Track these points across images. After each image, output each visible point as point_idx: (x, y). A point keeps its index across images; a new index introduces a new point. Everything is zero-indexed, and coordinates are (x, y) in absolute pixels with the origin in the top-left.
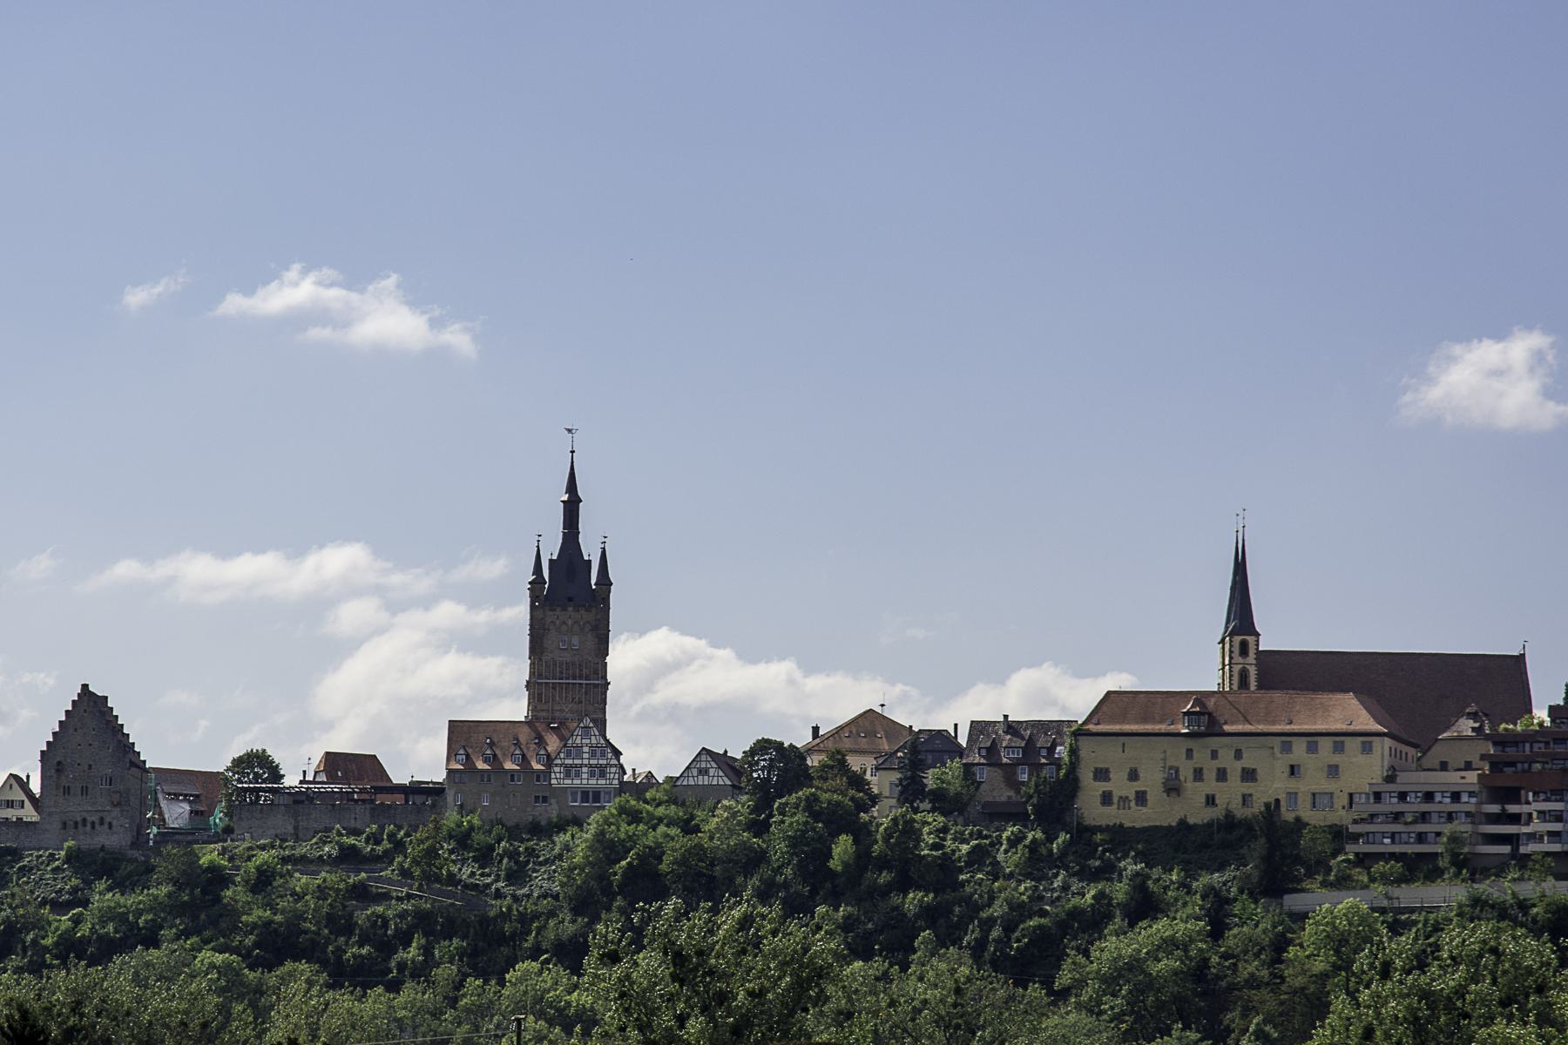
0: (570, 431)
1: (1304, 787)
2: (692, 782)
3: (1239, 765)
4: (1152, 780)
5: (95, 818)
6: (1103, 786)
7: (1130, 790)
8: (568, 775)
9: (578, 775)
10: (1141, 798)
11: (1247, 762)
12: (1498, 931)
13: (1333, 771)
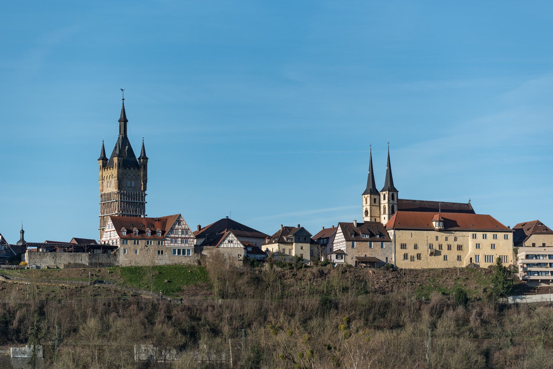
0: (122, 90)
1: (481, 254)
2: (225, 246)
3: (456, 243)
4: (424, 250)
6: (404, 251)
7: (414, 253)
8: (172, 242)
9: (176, 242)
10: (419, 256)
11: (459, 242)
12: (242, 307)
13: (493, 246)
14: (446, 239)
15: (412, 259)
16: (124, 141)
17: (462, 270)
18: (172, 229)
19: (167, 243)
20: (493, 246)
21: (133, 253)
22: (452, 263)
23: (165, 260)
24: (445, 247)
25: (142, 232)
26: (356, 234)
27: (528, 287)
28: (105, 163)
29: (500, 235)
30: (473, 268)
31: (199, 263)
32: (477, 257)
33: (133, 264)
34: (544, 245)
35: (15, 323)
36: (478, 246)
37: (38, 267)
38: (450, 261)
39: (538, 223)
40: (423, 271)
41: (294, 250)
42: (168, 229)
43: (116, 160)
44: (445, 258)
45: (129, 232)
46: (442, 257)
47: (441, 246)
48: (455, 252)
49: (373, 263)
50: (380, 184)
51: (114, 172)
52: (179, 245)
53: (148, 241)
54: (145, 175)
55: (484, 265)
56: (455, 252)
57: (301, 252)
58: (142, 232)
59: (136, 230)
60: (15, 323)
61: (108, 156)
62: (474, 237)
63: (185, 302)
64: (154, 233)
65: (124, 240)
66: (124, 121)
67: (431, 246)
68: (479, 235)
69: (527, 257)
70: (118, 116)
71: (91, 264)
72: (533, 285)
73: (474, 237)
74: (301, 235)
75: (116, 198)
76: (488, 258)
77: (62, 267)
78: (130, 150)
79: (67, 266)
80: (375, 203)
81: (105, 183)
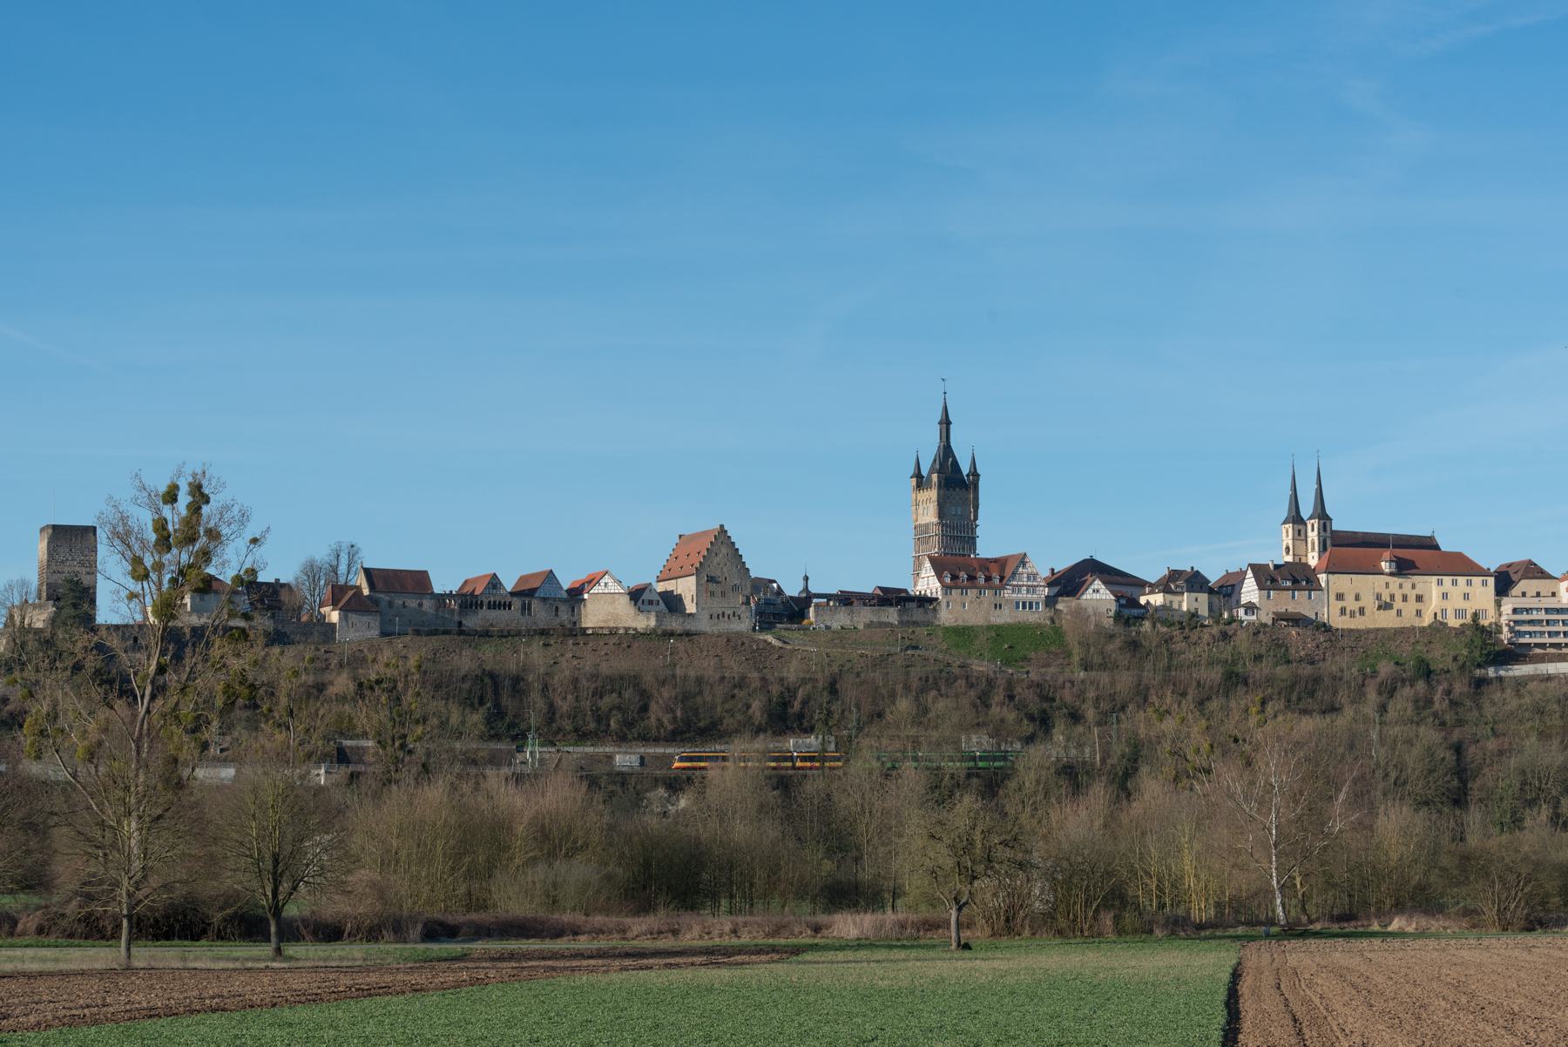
3: (1414, 592)
4: (1369, 602)
5: (728, 612)
6: (1341, 604)
7: (1355, 606)
10: (1362, 611)
11: (1418, 591)
12: (1113, 683)
13: (1466, 596)
14: (1401, 586)
15: (1352, 614)
16: (946, 451)
17: (1422, 630)
18: (1014, 574)
20: (1466, 596)
21: (960, 608)
22: (1409, 619)
23: (1004, 617)
24: (1398, 598)
25: (972, 578)
26: (1273, 580)
28: (921, 482)
29: (1477, 580)
30: (1438, 627)
31: (1053, 621)
32: (1444, 611)
33: (960, 623)
34: (1538, 595)
35: (797, 706)
36: (1445, 596)
37: (828, 628)
38: (1406, 616)
39: (1530, 562)
40: (1368, 631)
41: (1185, 602)
42: (1008, 573)
43: (935, 477)
44: (1399, 613)
45: (954, 577)
46: (1394, 612)
47: (1392, 597)
48: (1412, 606)
49: (1296, 620)
50: (1306, 510)
51: (932, 494)
52: (1024, 595)
53: (980, 588)
54: (976, 498)
55: (1453, 622)
56: (1412, 606)
57: (1196, 605)
58: (972, 578)
60: (797, 706)
61: (924, 472)
62: (1440, 583)
63: (1034, 676)
64: (988, 579)
65: (946, 588)
66: (946, 422)
67: (1379, 597)
68: (1447, 580)
69: (1515, 611)
70: (938, 416)
71: (901, 622)
72: (1523, 651)
73: (1440, 583)
74: (1195, 581)
75: (935, 530)
76: (1459, 613)
77: (861, 627)
78: (955, 464)
79: (869, 626)
80: (1300, 535)
81: (920, 511)
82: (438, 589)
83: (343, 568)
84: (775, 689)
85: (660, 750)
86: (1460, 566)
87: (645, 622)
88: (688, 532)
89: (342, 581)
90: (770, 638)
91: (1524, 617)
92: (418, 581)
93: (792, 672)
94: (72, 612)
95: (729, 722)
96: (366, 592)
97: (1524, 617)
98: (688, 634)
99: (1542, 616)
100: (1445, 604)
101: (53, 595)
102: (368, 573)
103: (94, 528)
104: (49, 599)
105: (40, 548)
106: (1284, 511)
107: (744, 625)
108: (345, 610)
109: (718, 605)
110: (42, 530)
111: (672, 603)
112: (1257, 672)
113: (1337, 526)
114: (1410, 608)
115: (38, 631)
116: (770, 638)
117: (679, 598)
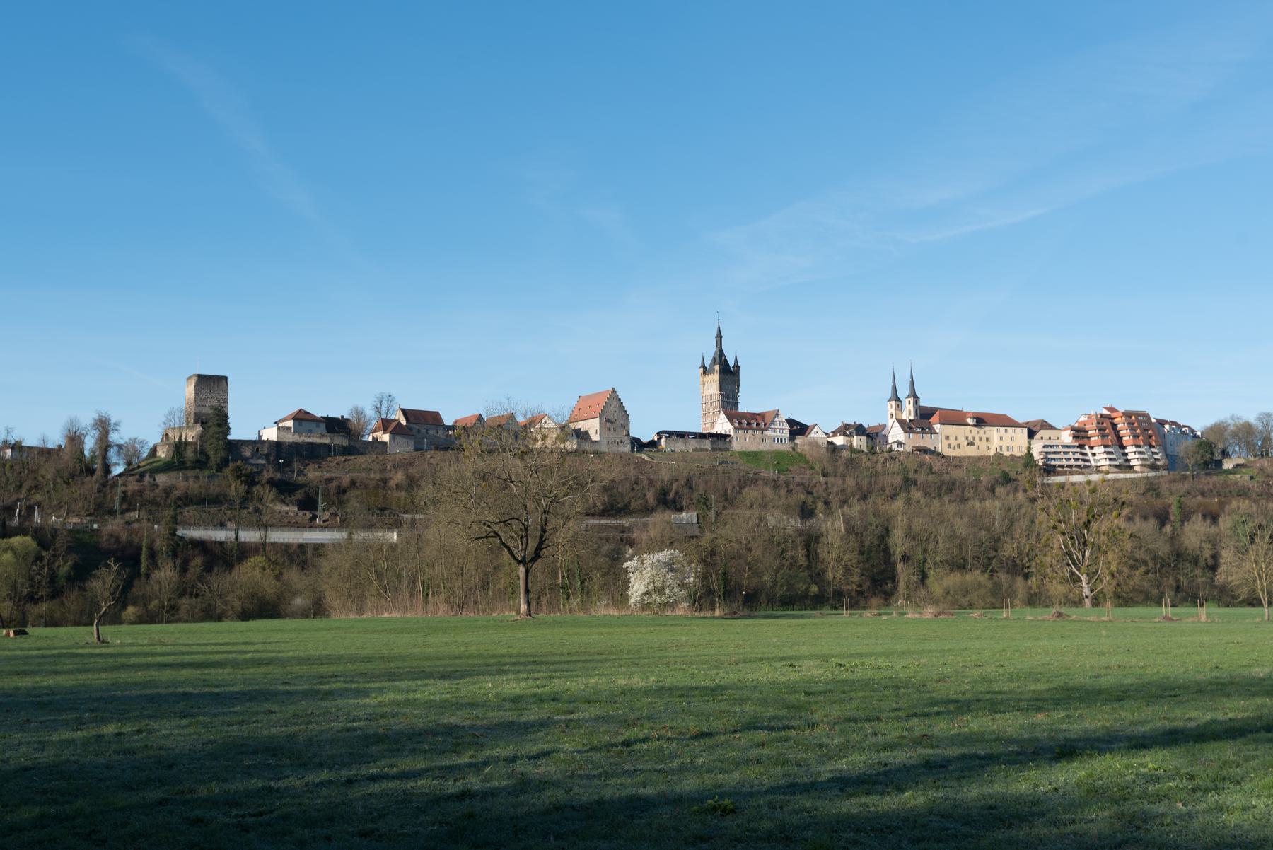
4: (963, 443)
10: (959, 446)
13: (1012, 439)
16: (721, 353)
17: (988, 457)
19: (769, 433)
20: (1012, 439)
22: (982, 451)
25: (749, 424)
27: (1049, 470)
28: (705, 371)
29: (1018, 430)
30: (999, 456)
35: (672, 496)
36: (1001, 438)
38: (979, 450)
43: (717, 367)
45: (740, 423)
49: (925, 450)
50: (903, 392)
51: (716, 377)
52: (777, 434)
55: (1006, 453)
58: (749, 424)
59: (744, 422)
60: (672, 496)
61: (707, 365)
63: (798, 480)
65: (736, 429)
66: (719, 337)
68: (1002, 429)
74: (860, 430)
80: (899, 407)
82: (448, 421)
83: (384, 409)
84: (658, 485)
85: (596, 522)
86: (1004, 422)
87: (571, 445)
88: (583, 394)
89: (384, 416)
90: (643, 456)
91: (1049, 450)
92: (434, 418)
93: (665, 475)
94: (217, 429)
95: (634, 505)
96: (404, 423)
97: (1049, 450)
98: (595, 453)
99: (1060, 449)
100: (1002, 443)
101: (199, 419)
102: (404, 411)
103: (226, 378)
104: (196, 422)
105: (190, 390)
106: (889, 394)
107: (627, 448)
108: (394, 434)
109: (612, 436)
110: (189, 379)
111: (582, 435)
112: (921, 478)
113: (922, 403)
114: (983, 444)
115: (195, 443)
116: (643, 456)
117: (586, 433)
